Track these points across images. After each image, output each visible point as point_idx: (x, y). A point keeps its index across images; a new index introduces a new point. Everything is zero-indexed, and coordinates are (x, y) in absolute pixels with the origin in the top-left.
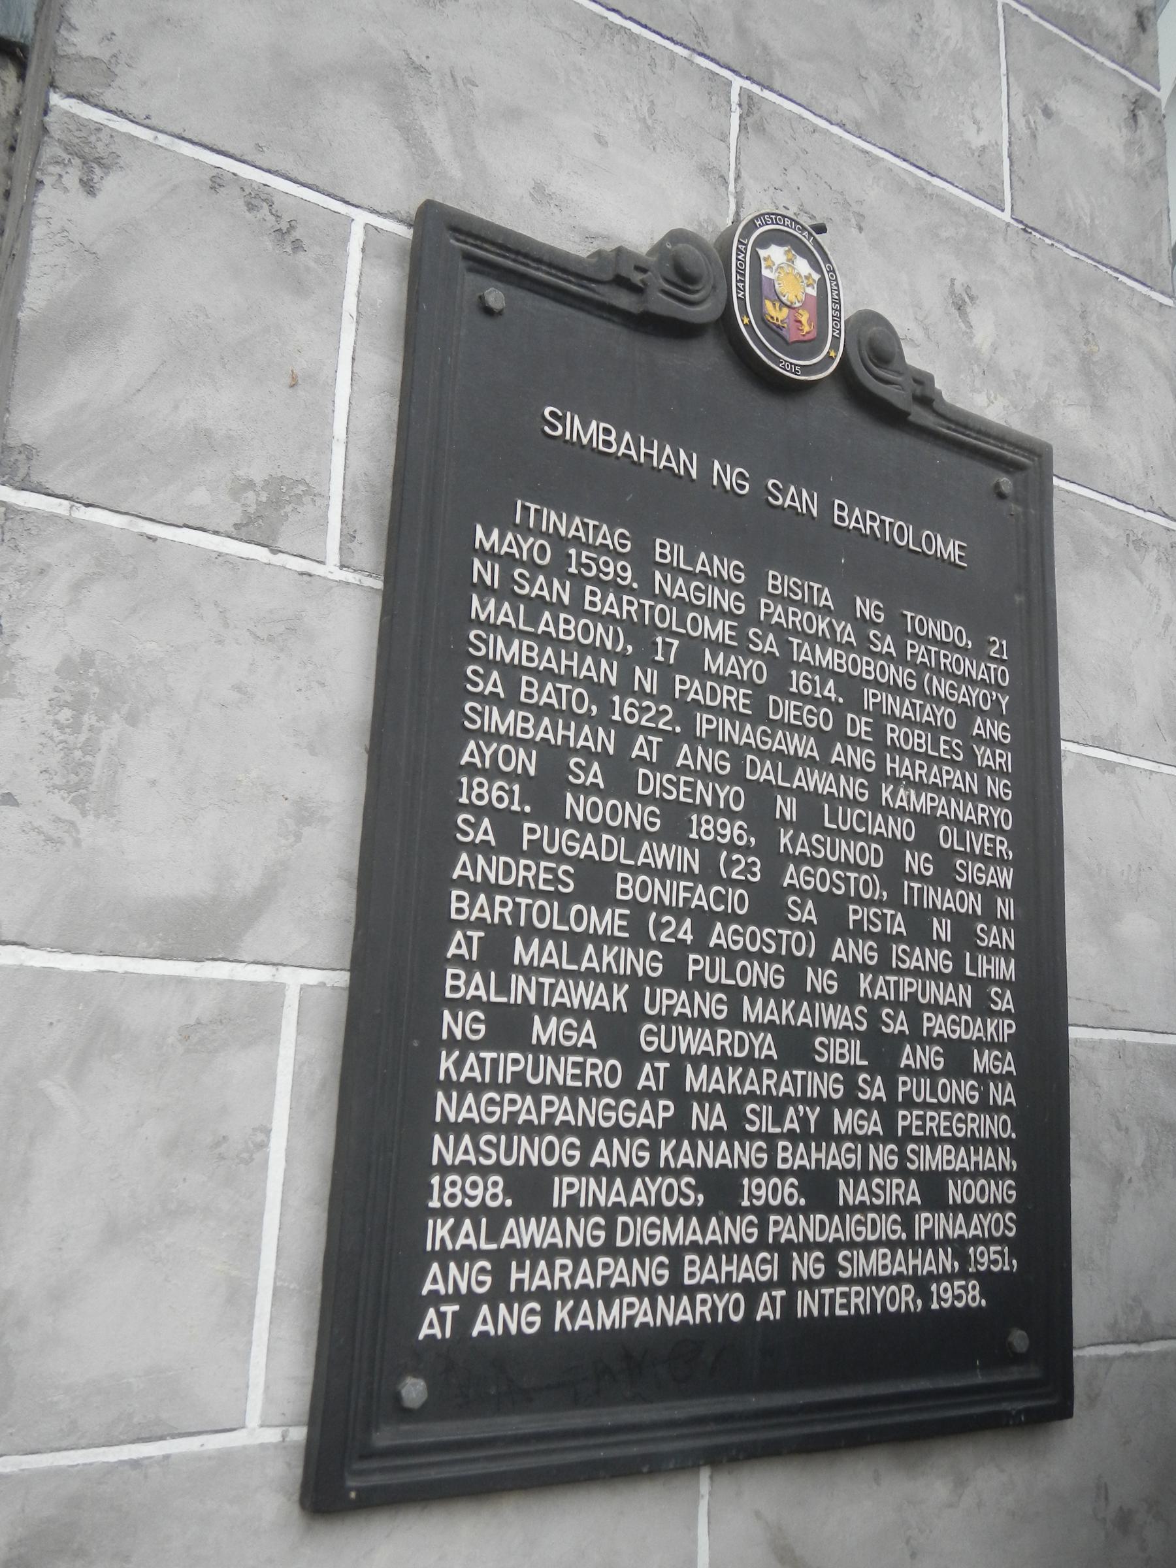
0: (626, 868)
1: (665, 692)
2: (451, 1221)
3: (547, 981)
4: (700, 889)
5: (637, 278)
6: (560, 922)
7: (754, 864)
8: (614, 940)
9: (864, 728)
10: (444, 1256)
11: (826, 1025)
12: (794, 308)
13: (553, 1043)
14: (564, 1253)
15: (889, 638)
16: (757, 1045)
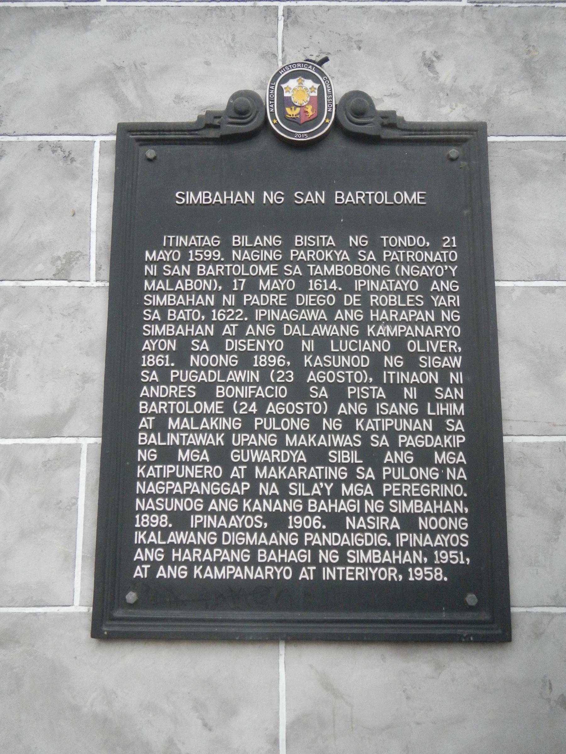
0: (221, 383)
1: (239, 303)
2: (145, 532)
3: (184, 435)
4: (260, 388)
5: (216, 122)
6: (189, 410)
7: (290, 374)
8: (215, 415)
9: (355, 300)
10: (143, 546)
11: (335, 445)
13: (188, 460)
14: (197, 546)
15: (371, 252)
16: (294, 456)
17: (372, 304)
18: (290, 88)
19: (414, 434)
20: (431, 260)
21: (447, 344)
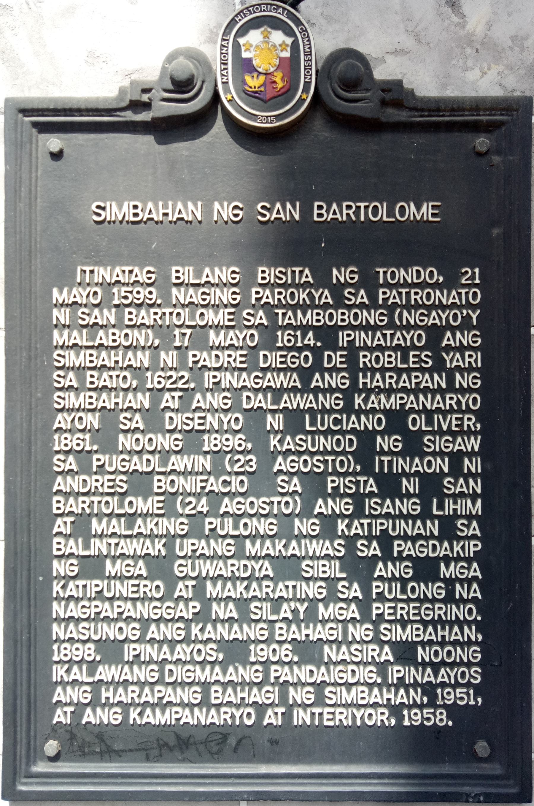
1: (182, 363)
3: (113, 541)
5: (145, 98)
7: (251, 460)
9: (339, 359)
12: (270, 74)
15: (362, 292)
16: (257, 567)
17: (361, 366)
18: (251, 45)
19: (414, 539)
20: (444, 302)
21: (462, 419)
